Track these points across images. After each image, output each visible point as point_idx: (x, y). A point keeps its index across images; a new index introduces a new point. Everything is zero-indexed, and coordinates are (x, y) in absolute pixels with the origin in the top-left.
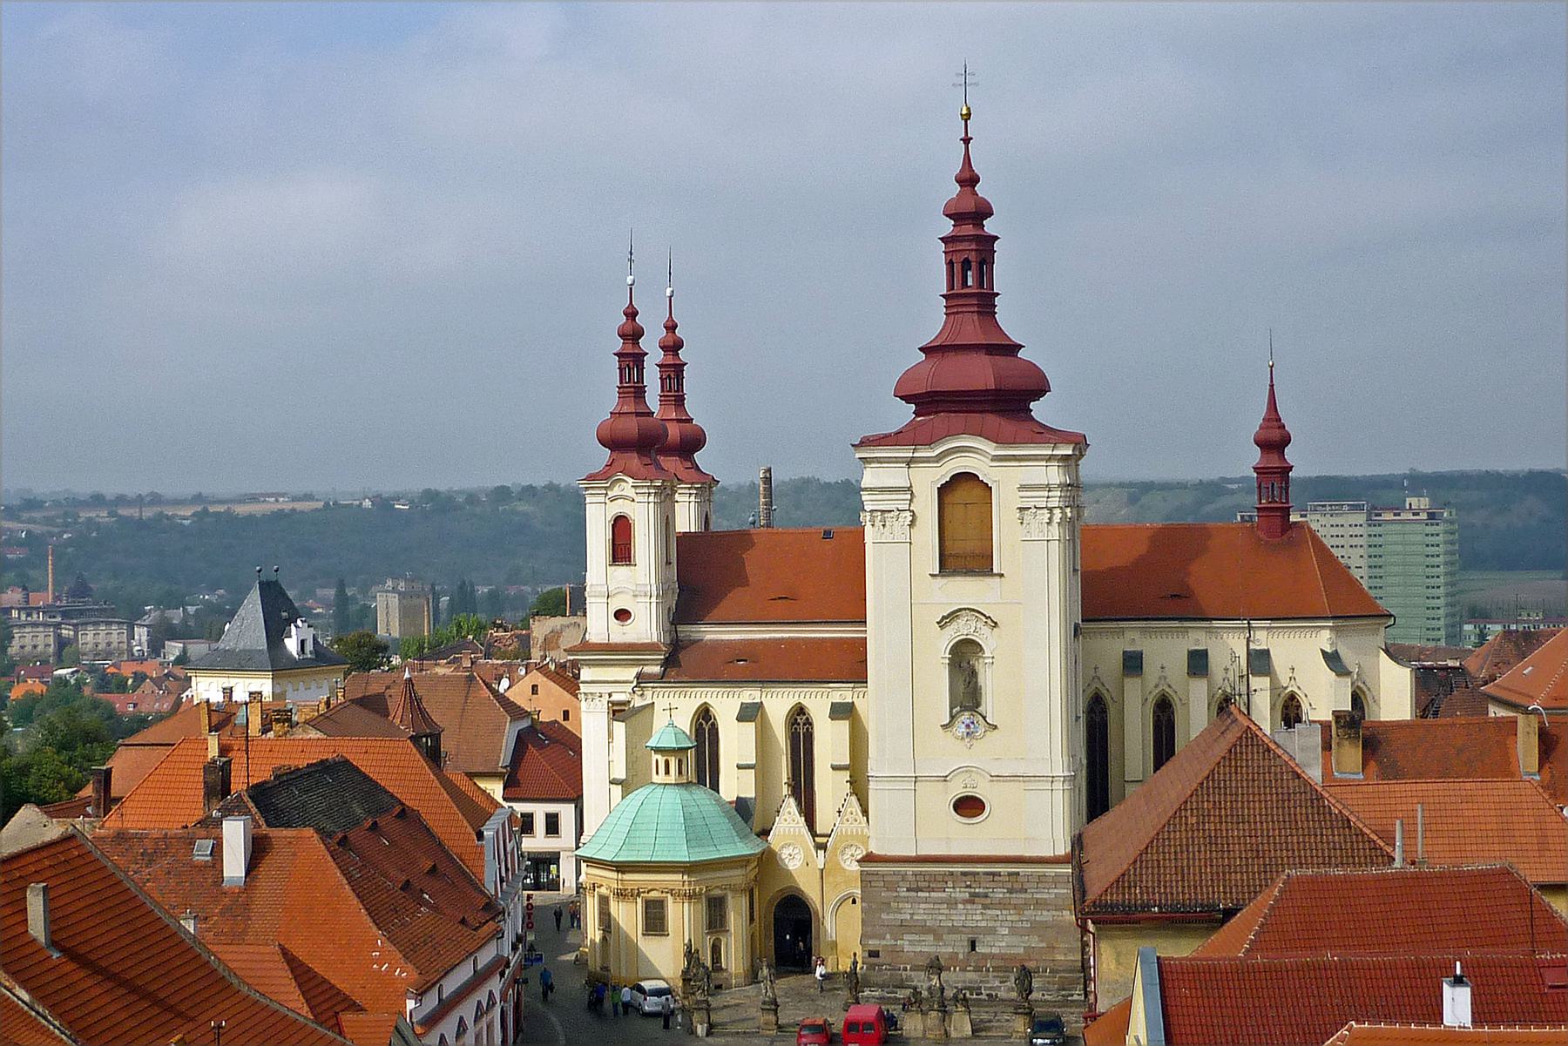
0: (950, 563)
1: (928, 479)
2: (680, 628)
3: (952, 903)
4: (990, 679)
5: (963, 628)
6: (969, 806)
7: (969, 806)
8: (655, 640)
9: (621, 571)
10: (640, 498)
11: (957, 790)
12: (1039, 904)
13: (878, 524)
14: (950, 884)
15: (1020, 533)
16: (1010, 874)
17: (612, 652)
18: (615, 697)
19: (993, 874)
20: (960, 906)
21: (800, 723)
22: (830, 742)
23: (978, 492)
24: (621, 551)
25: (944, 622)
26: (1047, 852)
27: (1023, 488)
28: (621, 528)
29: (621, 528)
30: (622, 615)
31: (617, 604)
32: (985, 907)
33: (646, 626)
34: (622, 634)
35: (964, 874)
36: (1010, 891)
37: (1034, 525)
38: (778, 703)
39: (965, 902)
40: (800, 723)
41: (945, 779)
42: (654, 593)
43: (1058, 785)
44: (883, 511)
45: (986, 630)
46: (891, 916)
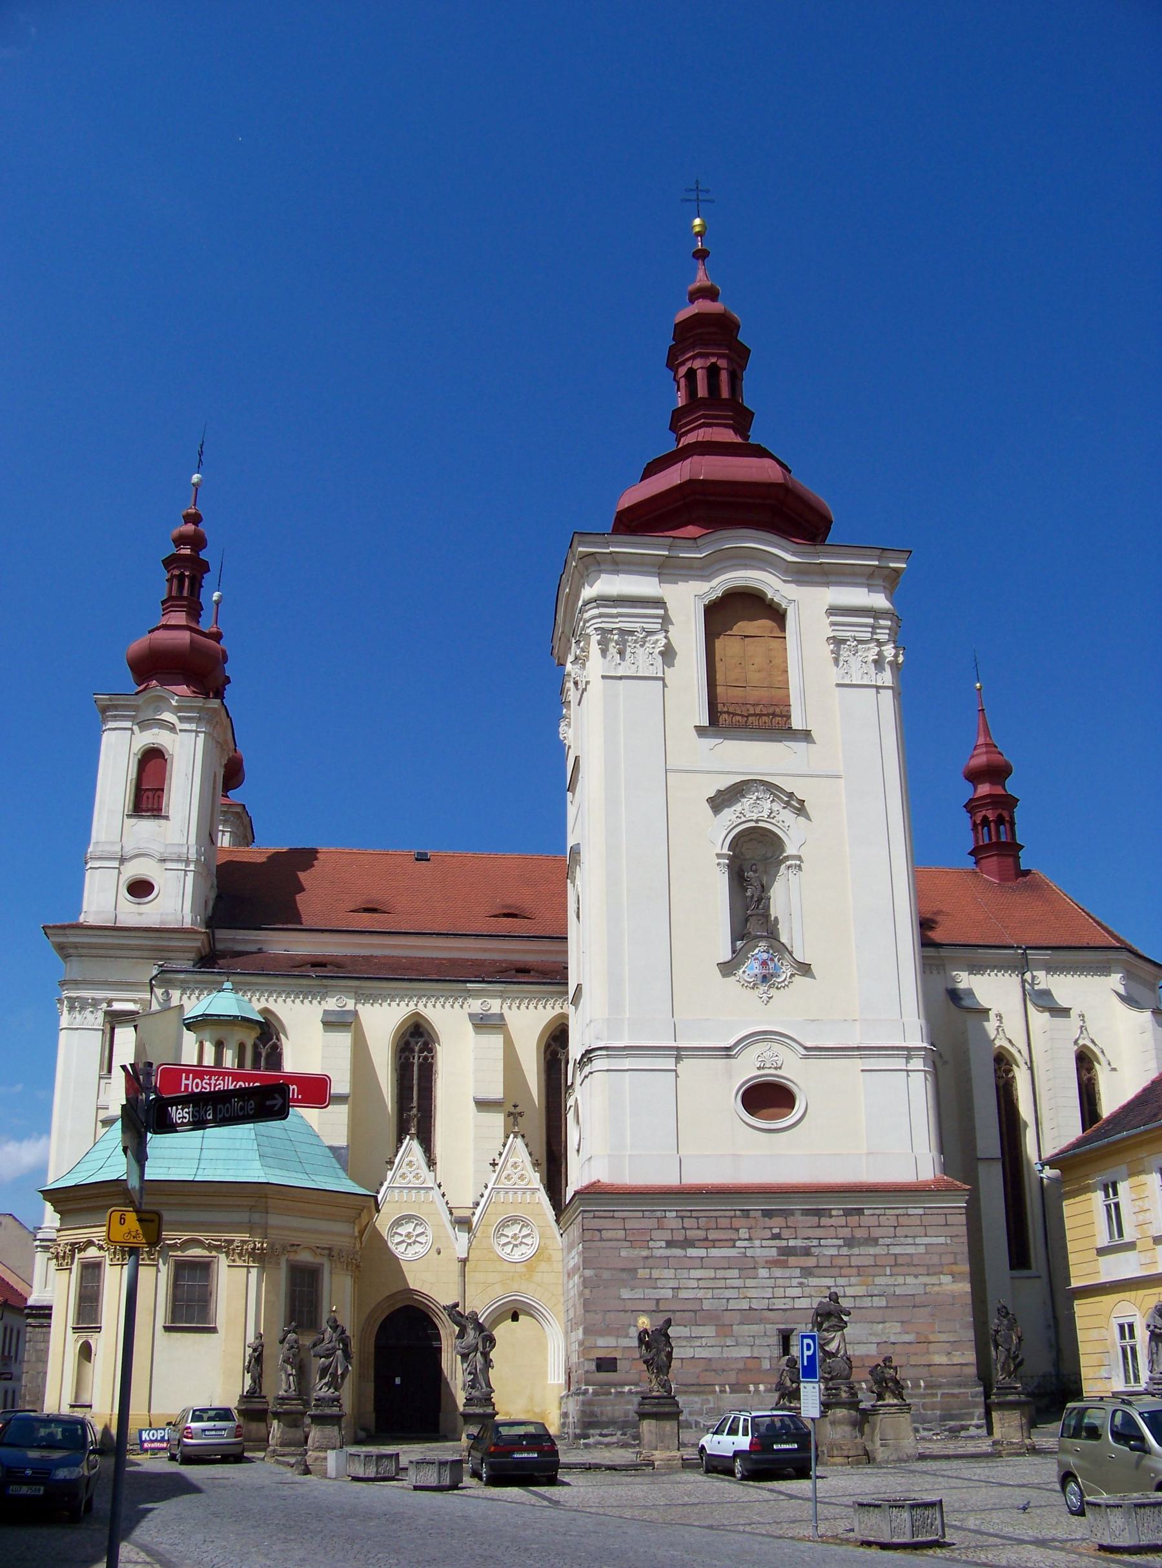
0: (725, 716)
1: (687, 600)
2: (221, 934)
3: (747, 1267)
4: (786, 896)
5: (751, 811)
6: (767, 1098)
7: (767, 1098)
8: (188, 924)
9: (146, 827)
10: (187, 726)
11: (748, 1068)
12: (896, 1262)
13: (613, 649)
14: (744, 1233)
15: (835, 675)
16: (848, 1213)
17: (116, 941)
18: (117, 1006)
19: (818, 1213)
20: (763, 1272)
21: (415, 1043)
22: (467, 1066)
23: (763, 625)
24: (147, 799)
25: (720, 801)
26: (903, 1174)
27: (833, 611)
28: (152, 761)
29: (152, 761)
30: (140, 889)
31: (134, 870)
32: (807, 1272)
33: (176, 903)
34: (133, 913)
35: (767, 1214)
36: (850, 1242)
37: (855, 663)
38: (383, 1019)
39: (771, 1264)
40: (415, 1043)
41: (727, 1052)
42: (193, 856)
43: (917, 1064)
44: (622, 632)
45: (787, 816)
46: (639, 1293)
